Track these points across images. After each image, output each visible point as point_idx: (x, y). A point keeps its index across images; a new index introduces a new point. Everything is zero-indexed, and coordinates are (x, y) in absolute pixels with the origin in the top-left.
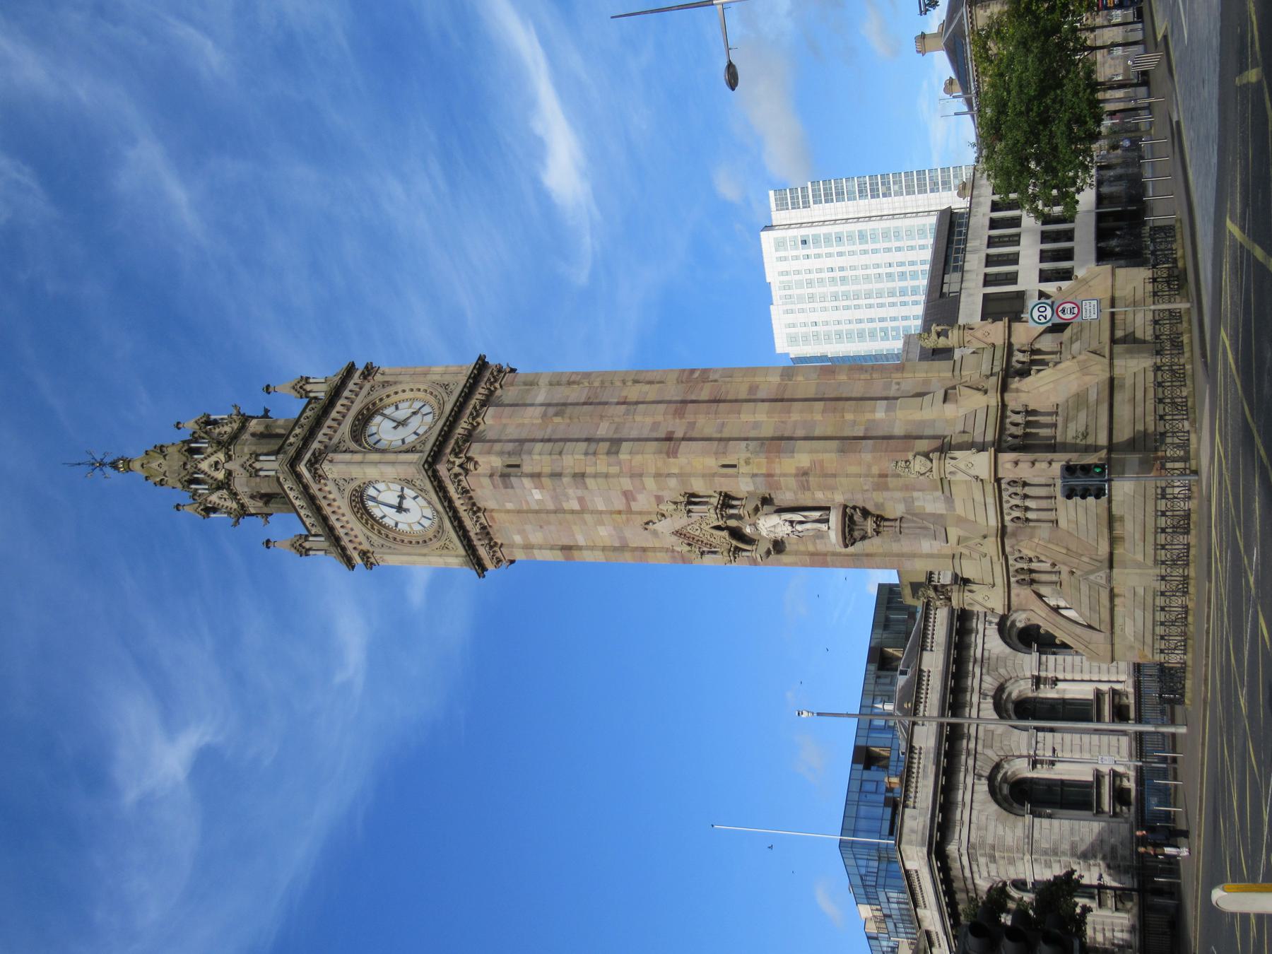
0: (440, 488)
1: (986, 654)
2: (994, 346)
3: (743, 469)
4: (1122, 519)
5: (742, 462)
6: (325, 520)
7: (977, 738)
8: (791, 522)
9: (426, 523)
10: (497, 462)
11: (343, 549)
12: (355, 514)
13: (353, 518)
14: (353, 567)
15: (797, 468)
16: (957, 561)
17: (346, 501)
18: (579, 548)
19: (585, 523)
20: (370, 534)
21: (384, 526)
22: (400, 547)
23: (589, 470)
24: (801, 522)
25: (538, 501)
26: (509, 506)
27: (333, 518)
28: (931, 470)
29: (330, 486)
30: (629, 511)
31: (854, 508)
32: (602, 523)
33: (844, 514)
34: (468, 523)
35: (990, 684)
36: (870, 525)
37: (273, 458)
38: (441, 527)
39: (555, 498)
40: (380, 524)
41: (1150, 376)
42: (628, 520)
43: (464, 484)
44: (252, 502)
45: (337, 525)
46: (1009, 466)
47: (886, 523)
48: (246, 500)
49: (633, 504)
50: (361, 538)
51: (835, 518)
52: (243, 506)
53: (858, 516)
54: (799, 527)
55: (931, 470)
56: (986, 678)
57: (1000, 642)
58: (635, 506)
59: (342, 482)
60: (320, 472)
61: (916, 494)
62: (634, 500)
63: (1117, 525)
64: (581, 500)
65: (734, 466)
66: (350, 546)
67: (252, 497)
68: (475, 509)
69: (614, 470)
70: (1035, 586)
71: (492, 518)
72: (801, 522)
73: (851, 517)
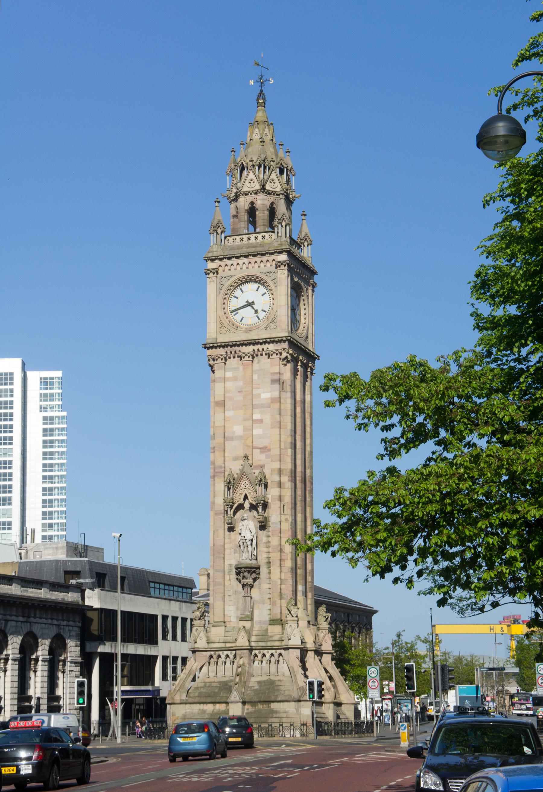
8: (252, 540)
13: (245, 274)
16: (223, 624)
17: (259, 274)
19: (245, 420)
20: (232, 280)
25: (259, 395)
26: (255, 377)
27: (246, 261)
31: (259, 573)
32: (245, 429)
36: (250, 581)
37: (288, 236)
42: (248, 446)
43: (274, 356)
44: (249, 201)
47: (249, 589)
48: (251, 198)
49: (258, 451)
51: (254, 562)
53: (254, 575)
54: (249, 543)
58: (256, 452)
59: (273, 277)
60: (282, 267)
62: (261, 452)
64: (261, 421)
66: (223, 263)
67: (252, 203)
70: (207, 664)
73: (254, 572)
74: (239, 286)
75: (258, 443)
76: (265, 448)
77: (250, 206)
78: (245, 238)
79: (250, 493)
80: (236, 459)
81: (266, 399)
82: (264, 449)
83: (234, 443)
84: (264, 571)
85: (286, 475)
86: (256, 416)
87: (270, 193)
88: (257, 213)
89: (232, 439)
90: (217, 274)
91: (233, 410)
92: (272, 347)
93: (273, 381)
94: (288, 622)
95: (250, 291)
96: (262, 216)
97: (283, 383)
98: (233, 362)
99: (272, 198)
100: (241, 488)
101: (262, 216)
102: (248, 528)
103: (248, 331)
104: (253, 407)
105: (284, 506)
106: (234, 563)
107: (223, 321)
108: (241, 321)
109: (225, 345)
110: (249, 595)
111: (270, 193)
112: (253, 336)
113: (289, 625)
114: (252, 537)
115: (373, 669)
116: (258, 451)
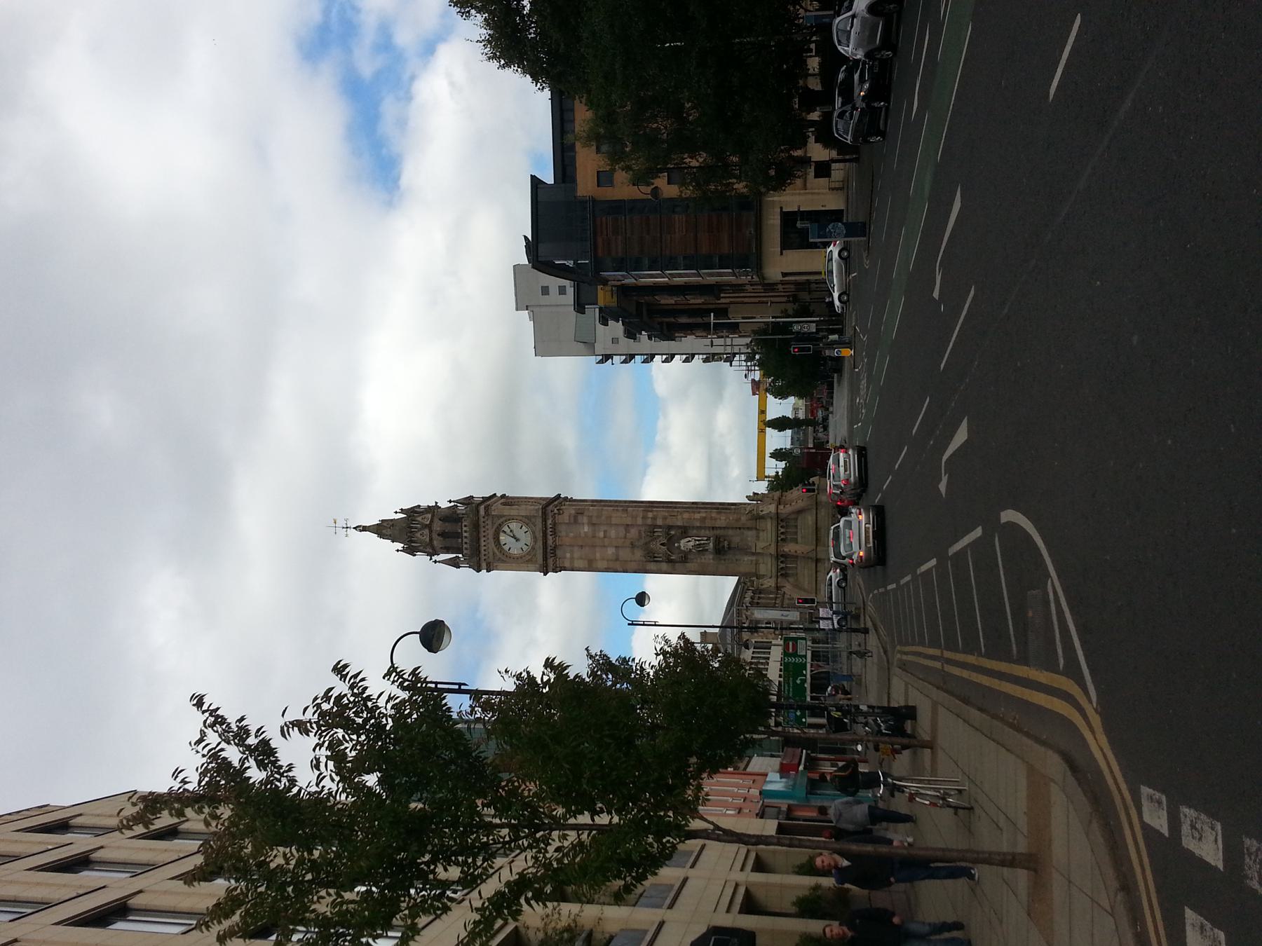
0: (545, 520)
9: (525, 548)
29: (489, 522)
38: (533, 548)
45: (483, 544)
48: (435, 536)
52: (431, 539)
66: (483, 558)
68: (554, 533)
75: (622, 534)
84: (718, 532)
86: (602, 534)
89: (617, 555)
92: (549, 522)
96: (449, 527)
98: (559, 553)
101: (449, 527)
103: (535, 542)
109: (545, 559)
111: (432, 521)
112: (540, 535)
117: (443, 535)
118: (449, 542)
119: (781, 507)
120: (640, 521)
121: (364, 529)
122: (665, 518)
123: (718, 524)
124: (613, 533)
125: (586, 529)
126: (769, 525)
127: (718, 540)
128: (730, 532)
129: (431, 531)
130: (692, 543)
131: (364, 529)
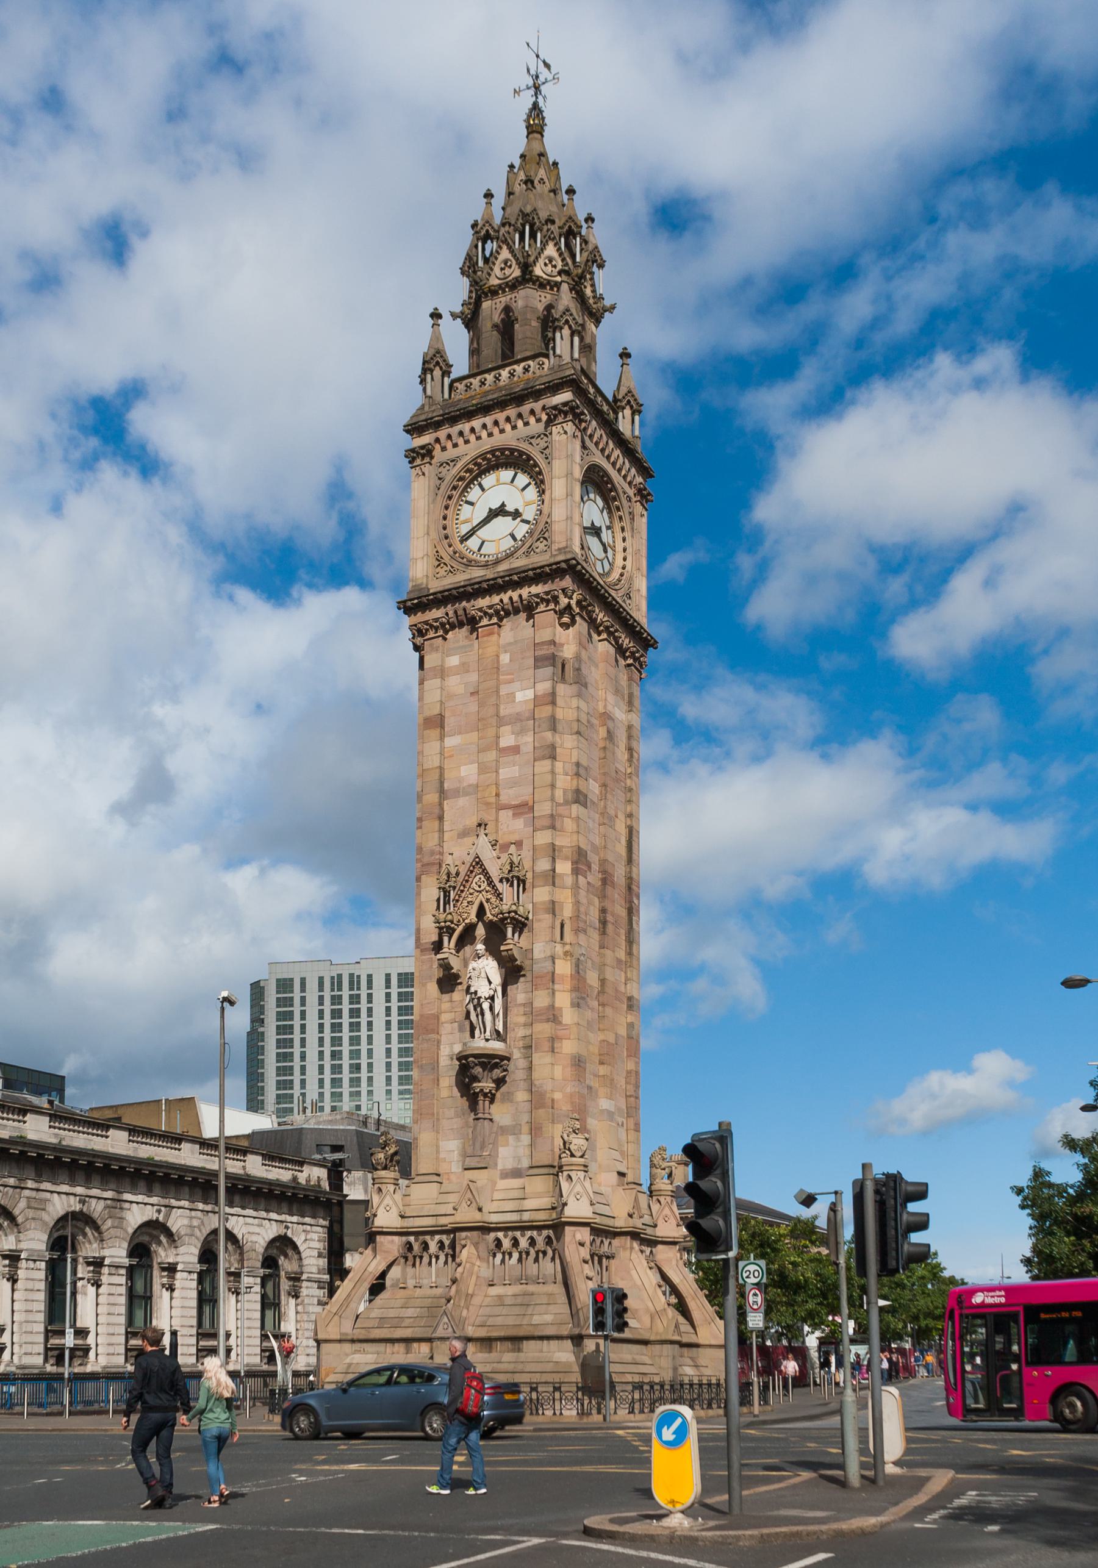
1: (127, 1205)
2: (655, 1226)
3: (559, 949)
4: (519, 1350)
5: (568, 947)
6: (485, 409)
7: (38, 1190)
8: (492, 998)
10: (568, 651)
11: (437, 425)
12: (492, 452)
14: (407, 431)
15: (561, 1009)
18: (442, 738)
20: (460, 465)
21: (468, 486)
22: (441, 501)
23: (559, 766)
24: (491, 1008)
28: (572, 1155)
30: (501, 807)
32: (482, 769)
33: (503, 1058)
34: (483, 602)
35: (96, 1208)
39: (517, 719)
40: (471, 482)
41: (657, 1379)
42: (488, 804)
44: (500, 307)
46: (579, 1237)
48: (503, 300)
49: (510, 813)
50: (451, 453)
51: (496, 1046)
52: (494, 292)
53: (497, 1073)
55: (572, 1155)
56: (102, 1203)
57: (140, 1222)
58: (505, 816)
61: (526, 1139)
63: (509, 1344)
64: (515, 750)
65: (562, 938)
66: (442, 434)
67: (507, 309)
68: (503, 614)
69: (559, 795)
71: (491, 634)
72: (491, 1008)
74: (475, 478)
75: (509, 796)
76: (524, 805)
77: (502, 316)
78: (490, 377)
79: (488, 900)
80: (464, 834)
81: (526, 702)
82: (523, 809)
83: (462, 801)
85: (566, 858)
86: (507, 739)
87: (542, 284)
88: (517, 326)
89: (457, 793)
90: (432, 458)
91: (460, 733)
93: (539, 662)
94: (565, 1168)
95: (503, 488)
97: (563, 666)
99: (548, 296)
100: (471, 891)
101: (526, 332)
102: (483, 975)
104: (501, 721)
105: (562, 926)
106: (457, 1048)
107: (442, 553)
108: (479, 550)
110: (487, 1116)
111: (542, 284)
113: (565, 1173)
114: (492, 993)
115: (752, 1268)
116: (510, 813)
117: (507, 327)
118: (492, 341)
119: (584, 1234)
120: (543, 838)
121: (535, 125)
122: (553, 908)
123: (541, 1059)
124: (508, 772)
125: (520, 696)
126: (536, 1200)
127: (492, 1062)
128: (521, 1096)
129: (514, 285)
130: (484, 991)
131: (535, 125)
